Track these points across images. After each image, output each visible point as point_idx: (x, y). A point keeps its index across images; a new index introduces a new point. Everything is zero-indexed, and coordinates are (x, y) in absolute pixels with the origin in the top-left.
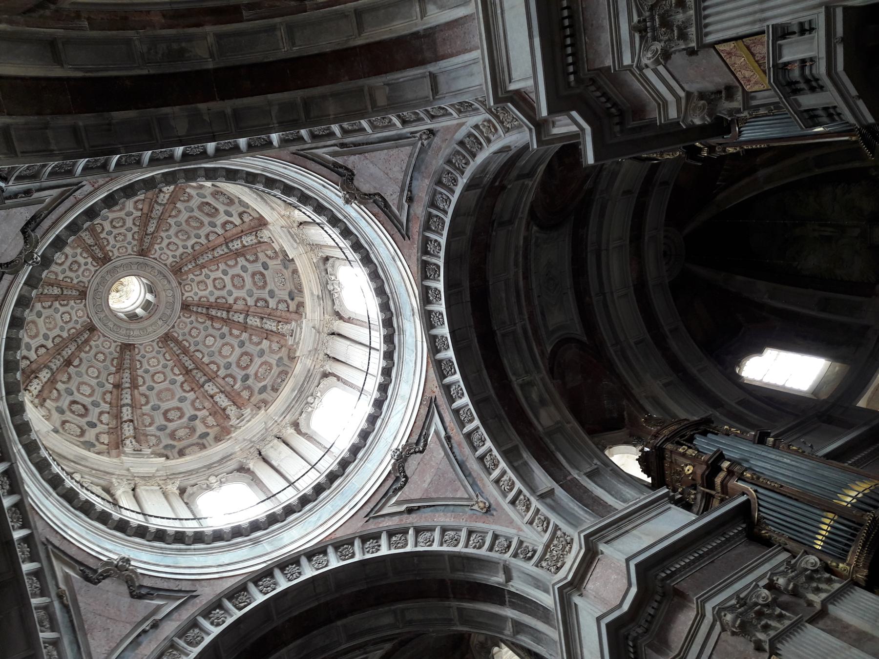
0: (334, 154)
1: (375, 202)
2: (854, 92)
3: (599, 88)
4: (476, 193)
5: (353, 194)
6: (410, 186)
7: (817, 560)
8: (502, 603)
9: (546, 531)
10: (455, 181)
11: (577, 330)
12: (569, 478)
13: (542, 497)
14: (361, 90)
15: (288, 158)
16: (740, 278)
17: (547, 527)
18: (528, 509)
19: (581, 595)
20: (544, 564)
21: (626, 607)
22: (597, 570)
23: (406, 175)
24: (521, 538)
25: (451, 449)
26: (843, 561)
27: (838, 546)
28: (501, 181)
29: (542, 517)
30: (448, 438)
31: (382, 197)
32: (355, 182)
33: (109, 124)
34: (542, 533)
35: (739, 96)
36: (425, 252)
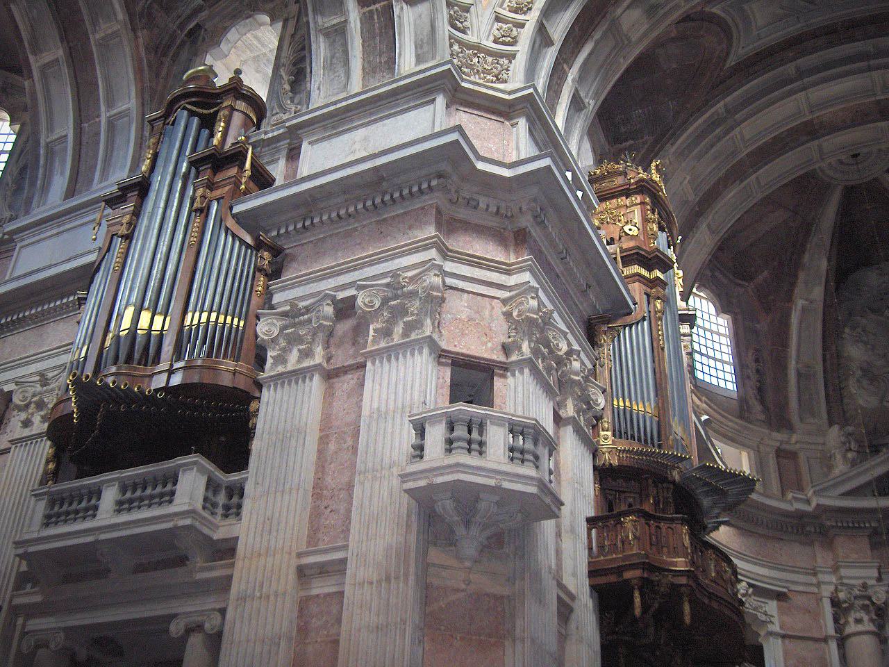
7: (602, 406)
9: (495, 41)
11: (742, 49)
12: (565, 66)
13: (541, 29)
16: (824, 264)
17: (504, 43)
18: (515, 11)
19: (448, 106)
20: (456, 47)
21: (481, 166)
22: (489, 123)
24: (472, 9)
26: (618, 434)
27: (625, 426)
29: (514, 33)
34: (492, 38)
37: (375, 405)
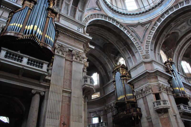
0: (147, 26)
1: (135, 26)
2: (164, 107)
3: (154, 75)
4: (130, 43)
5: (139, 24)
6: (134, 33)
8: (72, 4)
10: (134, 41)
14: (155, 39)
15: (152, 20)
23: (137, 33)
25: (93, 9)
28: (126, 46)
30: (95, 9)
31: (136, 27)
32: (140, 25)
33: (183, 10)
35: (152, 92)
36: (124, 28)
37: (75, 69)
